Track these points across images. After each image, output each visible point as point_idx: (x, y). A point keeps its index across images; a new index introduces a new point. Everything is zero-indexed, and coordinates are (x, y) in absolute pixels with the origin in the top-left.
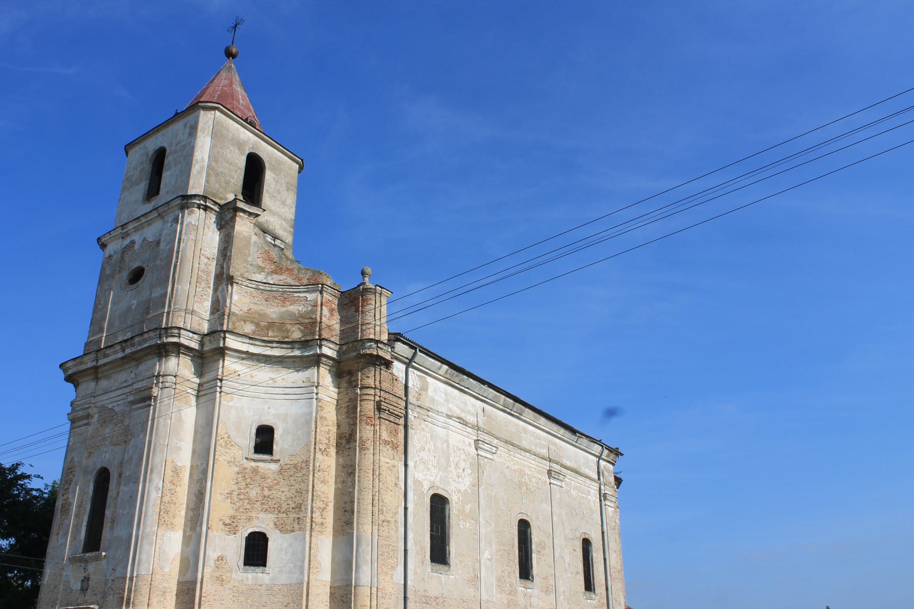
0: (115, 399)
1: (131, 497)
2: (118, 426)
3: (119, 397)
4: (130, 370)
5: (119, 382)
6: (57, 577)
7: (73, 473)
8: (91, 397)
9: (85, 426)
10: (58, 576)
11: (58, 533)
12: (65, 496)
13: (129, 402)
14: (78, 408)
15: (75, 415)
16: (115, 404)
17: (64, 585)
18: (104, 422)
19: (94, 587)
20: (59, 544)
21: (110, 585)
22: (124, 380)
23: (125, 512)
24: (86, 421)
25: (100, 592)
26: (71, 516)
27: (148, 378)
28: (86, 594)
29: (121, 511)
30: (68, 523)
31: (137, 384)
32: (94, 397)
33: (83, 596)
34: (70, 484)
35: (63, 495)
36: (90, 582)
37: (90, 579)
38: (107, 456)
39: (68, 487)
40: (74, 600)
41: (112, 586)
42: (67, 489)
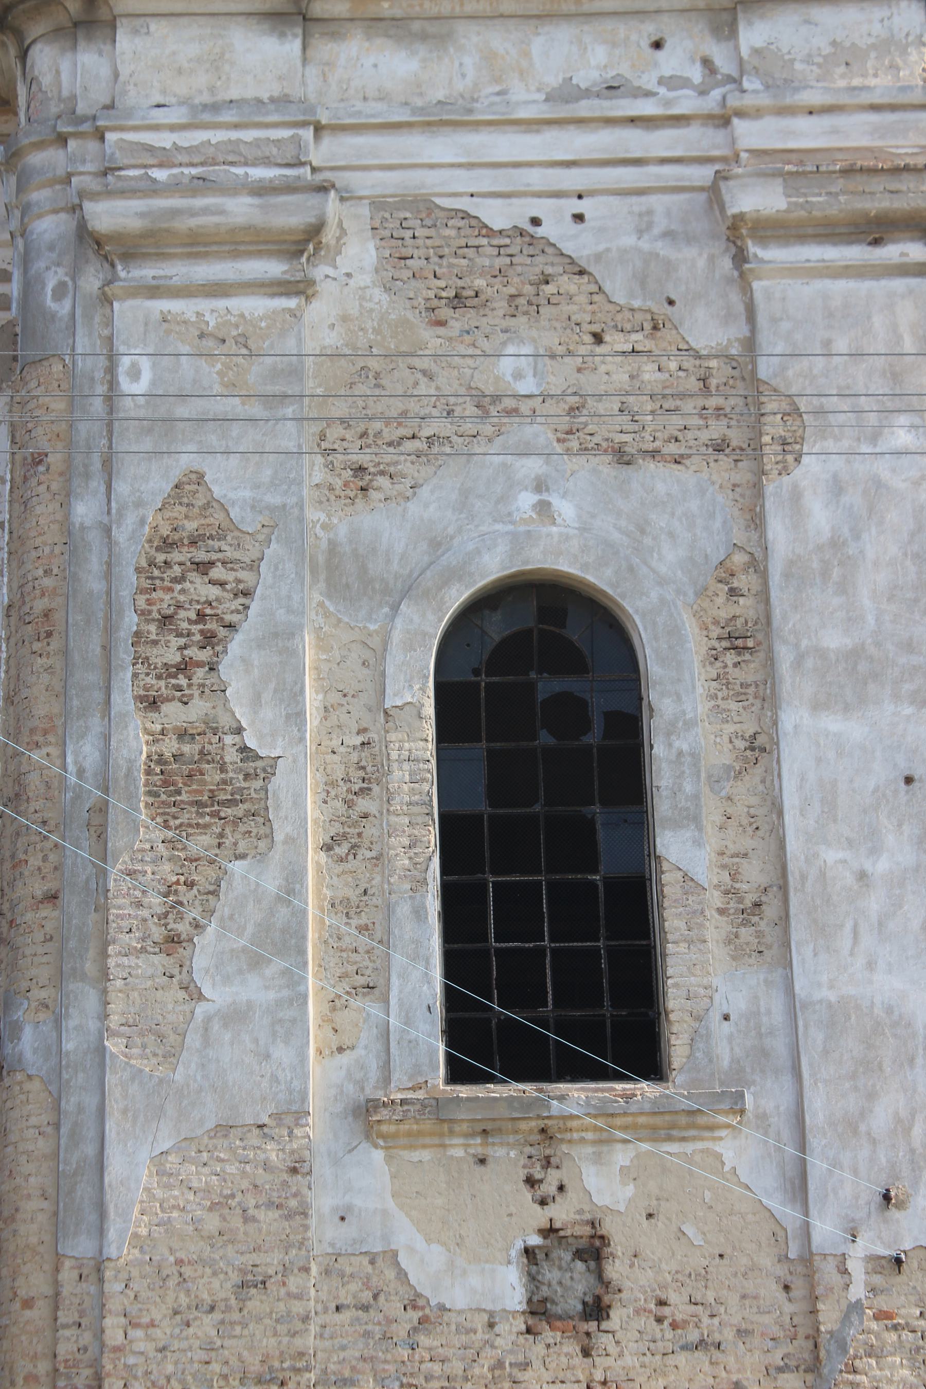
0: (536, 178)
1: (909, 780)
2: (616, 341)
3: (574, 172)
4: (649, 29)
5: (553, 80)
6: (247, 1219)
7: (217, 572)
8: (304, 124)
9: (287, 294)
10: (268, 1217)
11: (173, 941)
12: (165, 708)
13: (739, 218)
14: (160, 175)
15: (175, 213)
16: (538, 207)
17: (327, 1272)
18: (458, 301)
19: (673, 1297)
20: (201, 1009)
21: (857, 1291)
22: (585, 78)
23: (881, 866)
24: (274, 268)
25: (742, 1333)
26: (296, 842)
27: (875, 108)
28: (605, 1340)
29: (831, 856)
30: (271, 883)
31: (770, 123)
32: (319, 129)
33: (572, 1347)
34: (209, 639)
35: (152, 703)
36: (615, 1270)
37: (619, 1245)
38: (565, 509)
39: (203, 655)
40: (482, 1369)
41: (883, 1303)
42: (184, 667)
